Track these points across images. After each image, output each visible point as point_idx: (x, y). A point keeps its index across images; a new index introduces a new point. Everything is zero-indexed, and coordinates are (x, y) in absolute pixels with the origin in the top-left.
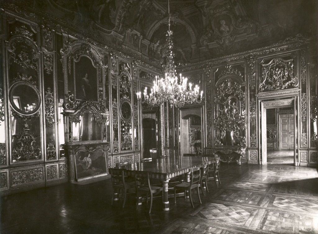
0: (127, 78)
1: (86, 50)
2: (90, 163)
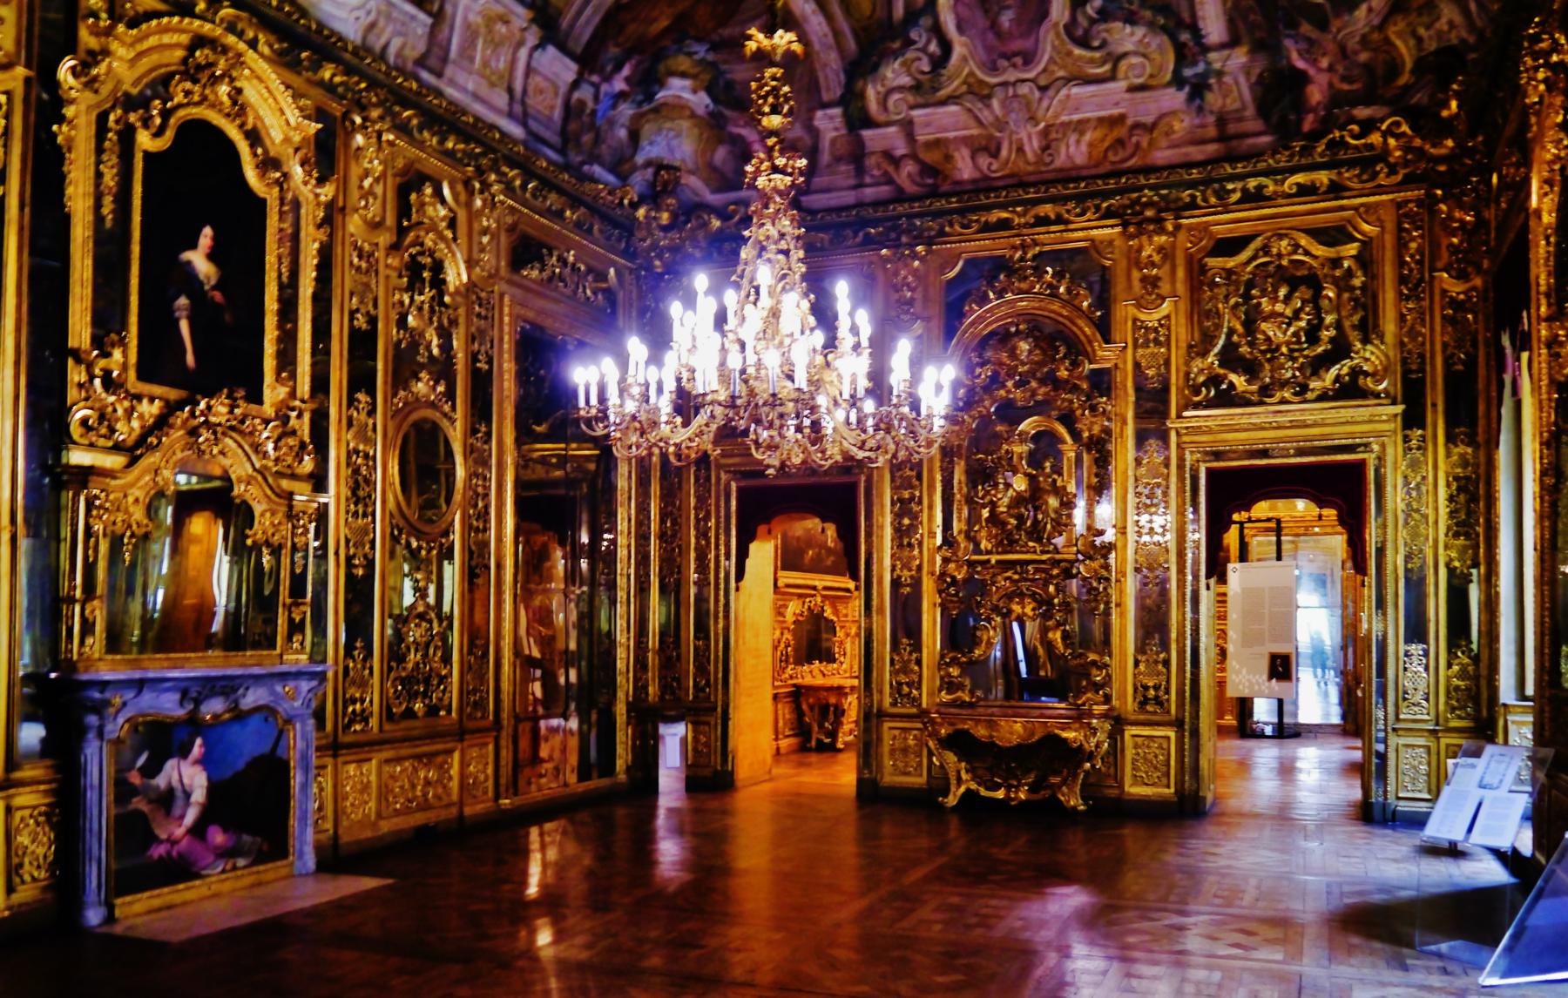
0: (438, 267)
1: (215, 81)
2: (199, 796)
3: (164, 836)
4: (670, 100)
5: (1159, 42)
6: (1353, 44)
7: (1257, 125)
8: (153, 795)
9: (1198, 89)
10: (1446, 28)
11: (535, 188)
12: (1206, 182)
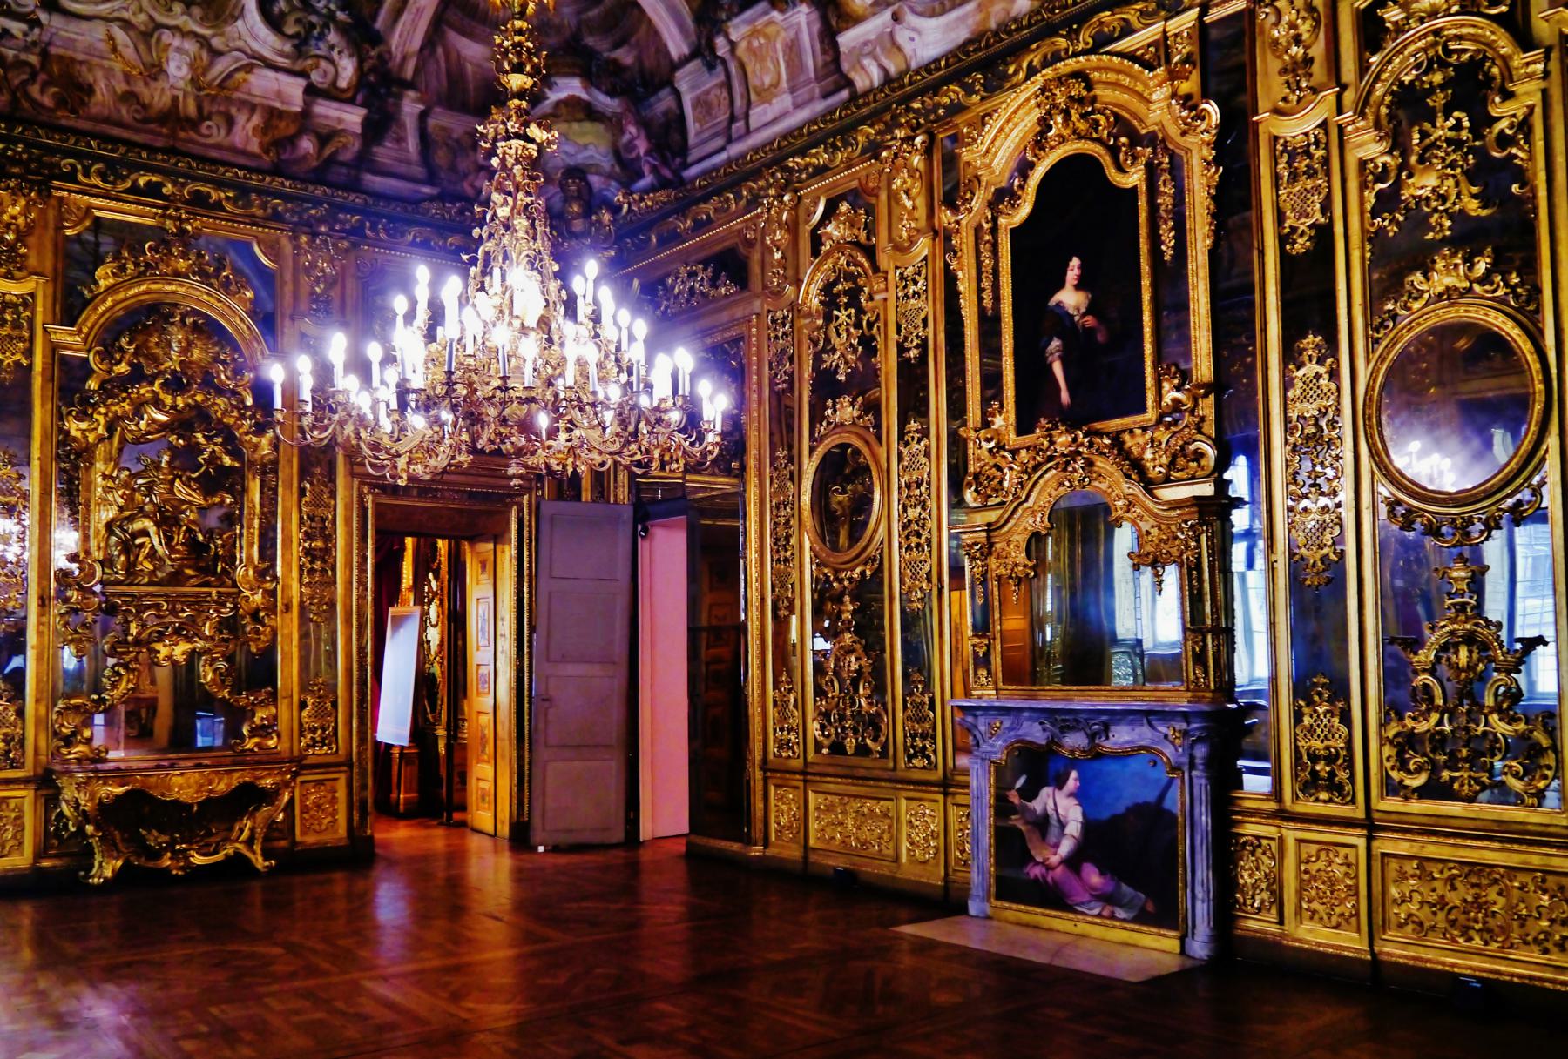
2: (1074, 829)
3: (1039, 859)
8: (1028, 817)
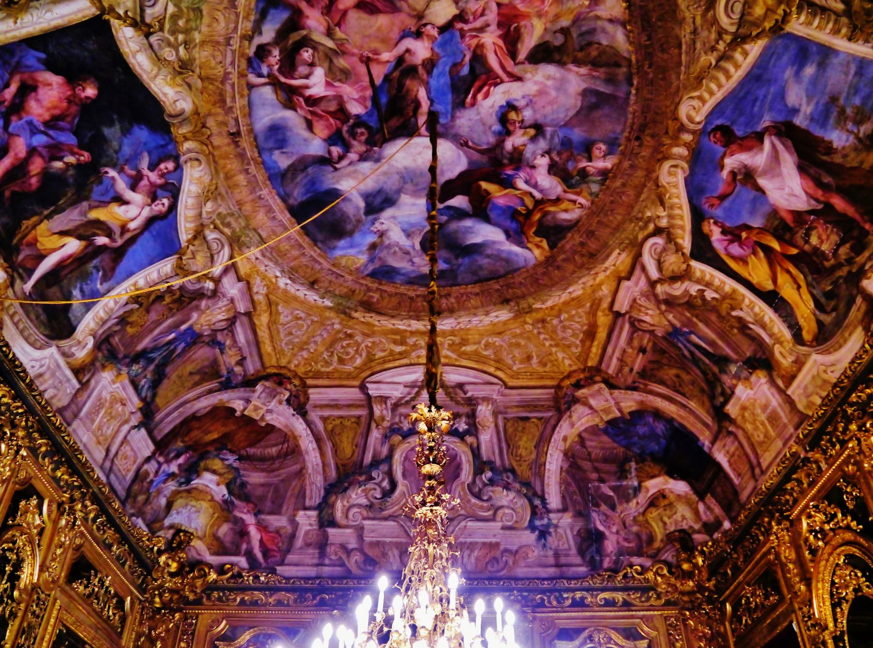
0: (18, 565)
4: (200, 487)
5: (522, 502)
6: (629, 520)
7: (578, 560)
9: (543, 534)
10: (680, 519)
11: (102, 523)
12: (551, 591)
